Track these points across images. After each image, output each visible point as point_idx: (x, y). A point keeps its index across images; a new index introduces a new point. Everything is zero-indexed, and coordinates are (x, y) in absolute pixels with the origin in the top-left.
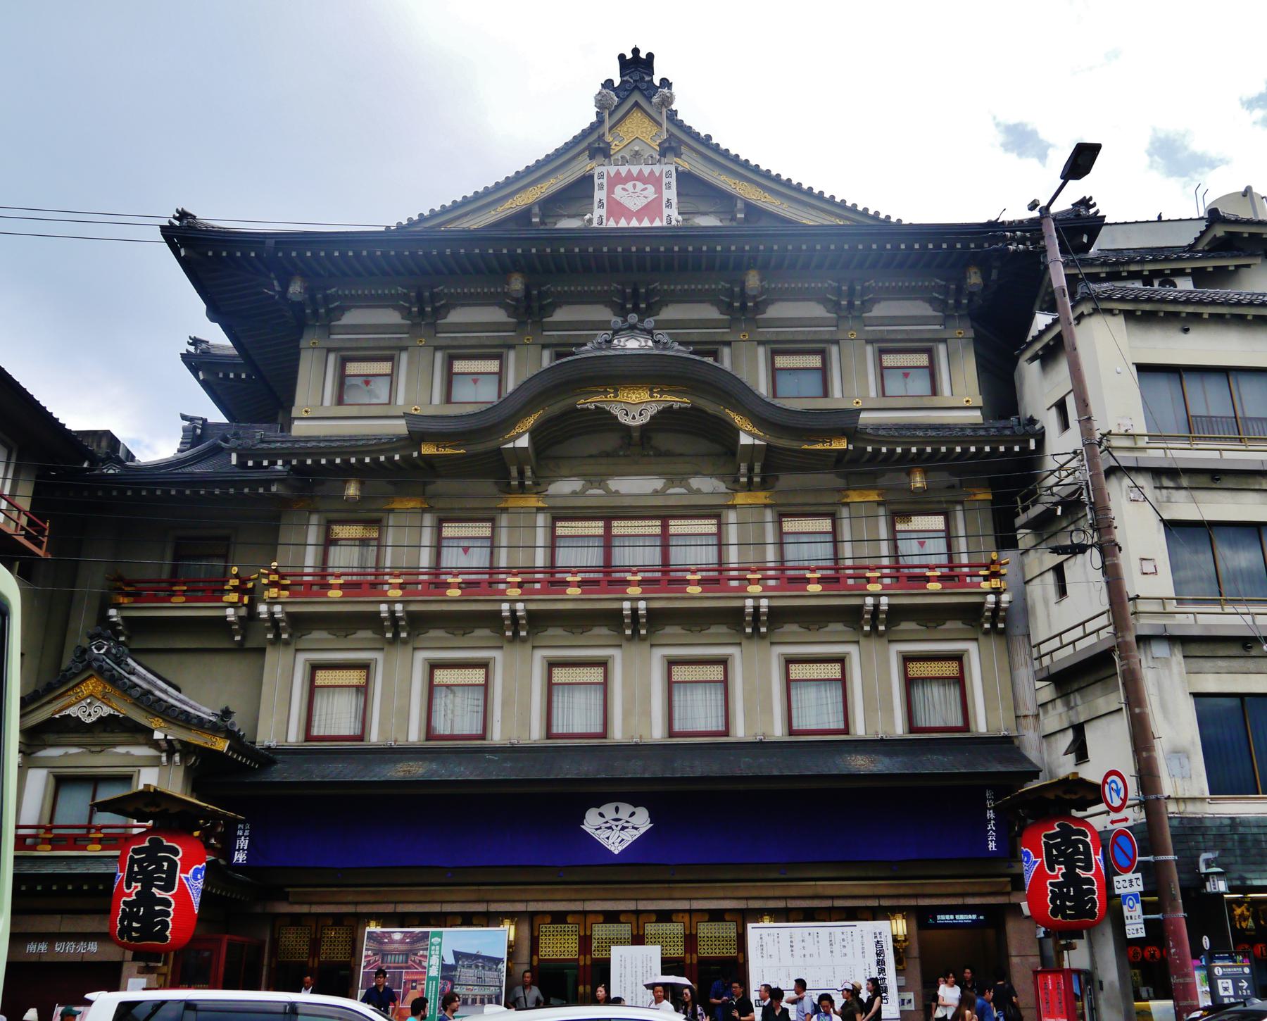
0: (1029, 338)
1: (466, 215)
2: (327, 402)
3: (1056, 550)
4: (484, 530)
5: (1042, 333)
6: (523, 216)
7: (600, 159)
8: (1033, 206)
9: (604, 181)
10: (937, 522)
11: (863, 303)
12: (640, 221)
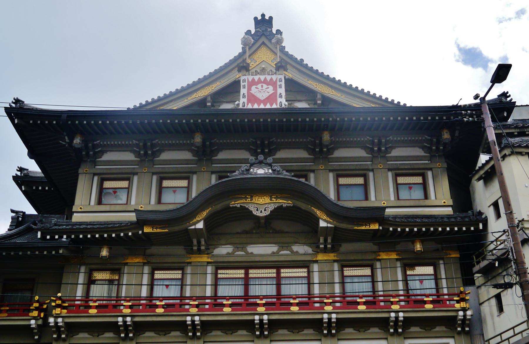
0: (477, 168)
1: (171, 101)
2: (93, 202)
3: (496, 286)
4: (177, 275)
5: (484, 165)
6: (202, 102)
7: (244, 72)
8: (476, 97)
9: (246, 84)
10: (430, 270)
11: (386, 149)
12: (265, 105)
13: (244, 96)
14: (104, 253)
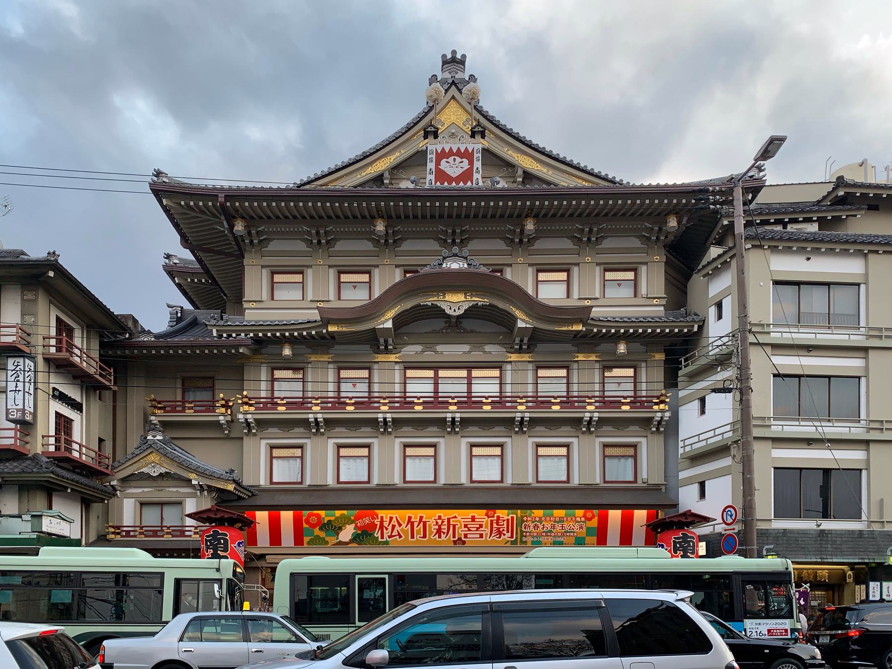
4: (365, 373)
10: (630, 372)
14: (287, 351)
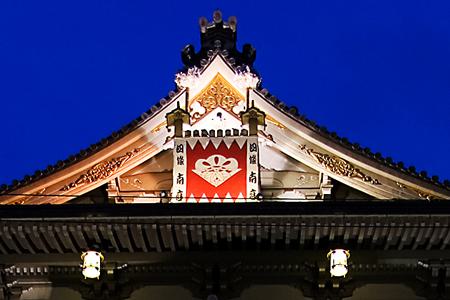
13: (180, 181)
